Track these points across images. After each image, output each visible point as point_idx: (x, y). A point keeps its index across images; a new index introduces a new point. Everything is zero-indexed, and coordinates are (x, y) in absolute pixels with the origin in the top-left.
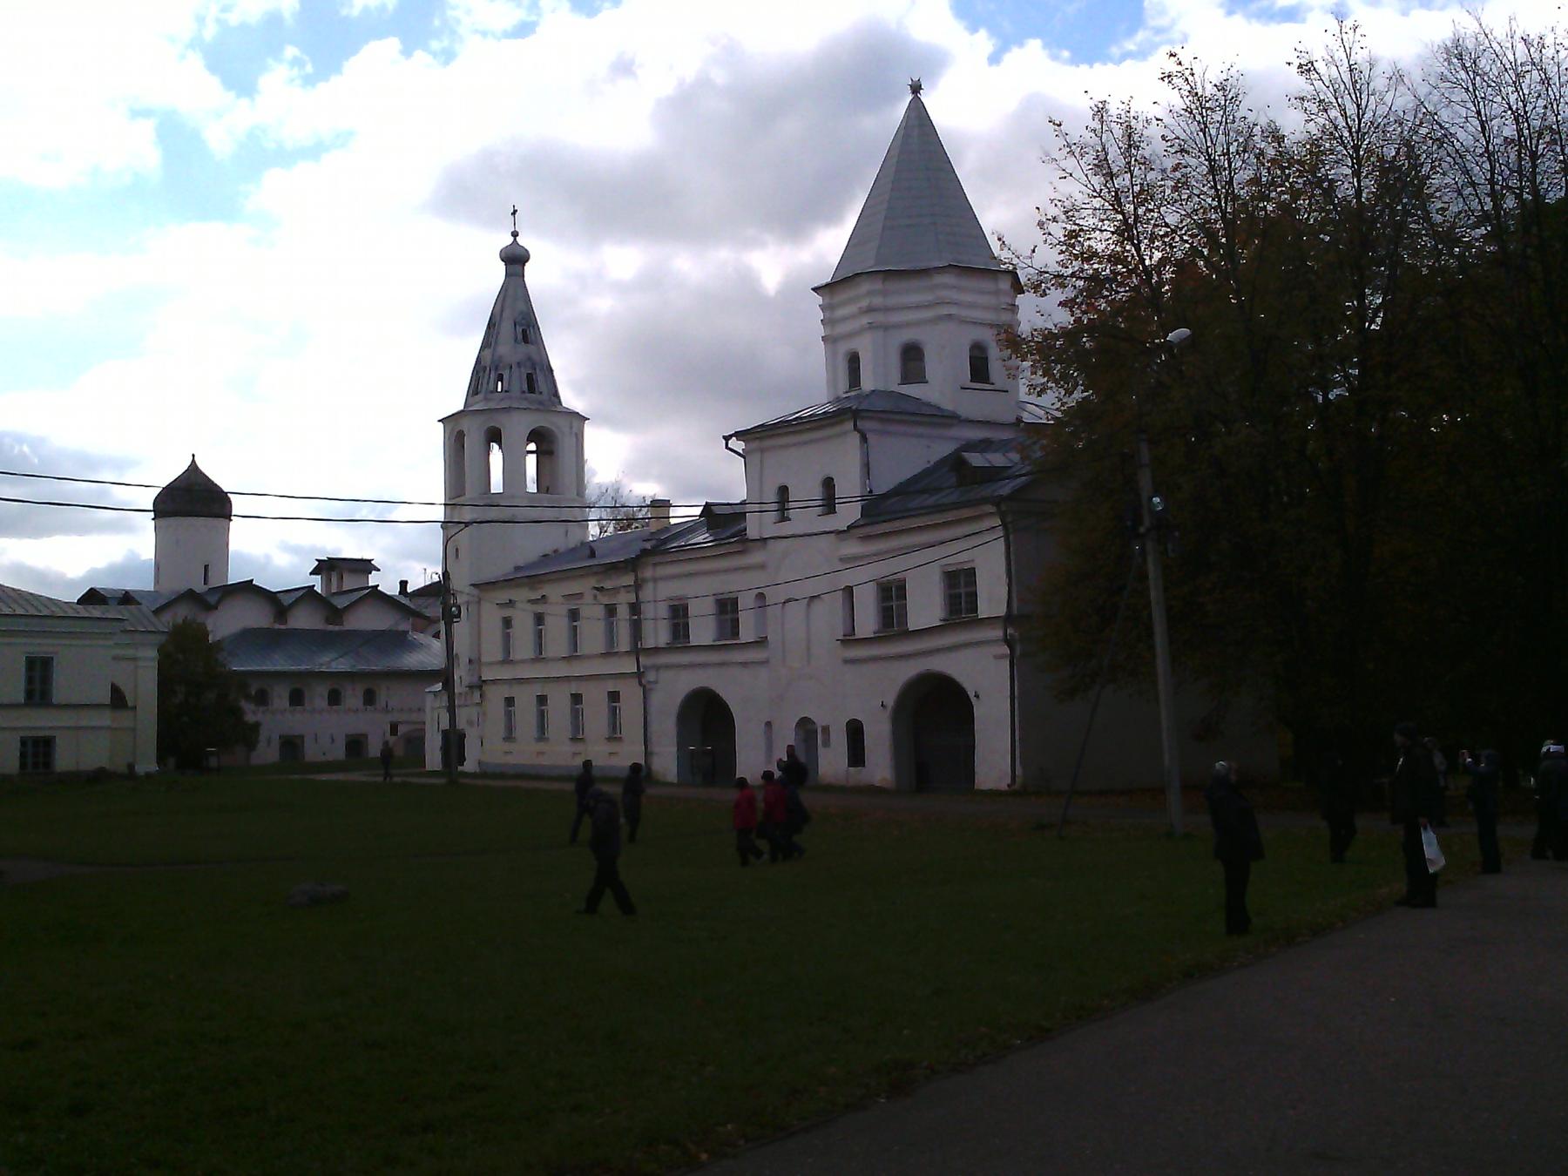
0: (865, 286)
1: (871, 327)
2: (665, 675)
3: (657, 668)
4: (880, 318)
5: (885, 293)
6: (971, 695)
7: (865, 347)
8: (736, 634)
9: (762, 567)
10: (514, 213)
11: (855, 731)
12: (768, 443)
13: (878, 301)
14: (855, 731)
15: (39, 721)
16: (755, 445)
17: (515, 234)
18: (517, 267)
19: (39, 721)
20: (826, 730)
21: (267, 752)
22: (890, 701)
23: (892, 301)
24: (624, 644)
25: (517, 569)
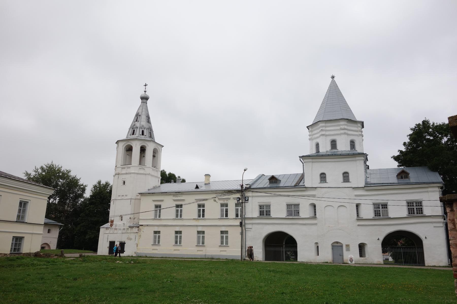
0: (342, 123)
1: (345, 134)
2: (255, 226)
3: (252, 224)
4: (346, 131)
5: (347, 125)
6: (422, 236)
7: (319, 141)
8: (298, 215)
9: (314, 196)
10: (146, 85)
11: (362, 247)
12: (314, 160)
13: (346, 127)
14: (362, 247)
15: (19, 229)
16: (311, 160)
17: (145, 92)
18: (145, 101)
19: (19, 229)
20: (348, 246)
21: (103, 249)
22: (382, 239)
23: (349, 128)
24: (232, 214)
25: (149, 190)
